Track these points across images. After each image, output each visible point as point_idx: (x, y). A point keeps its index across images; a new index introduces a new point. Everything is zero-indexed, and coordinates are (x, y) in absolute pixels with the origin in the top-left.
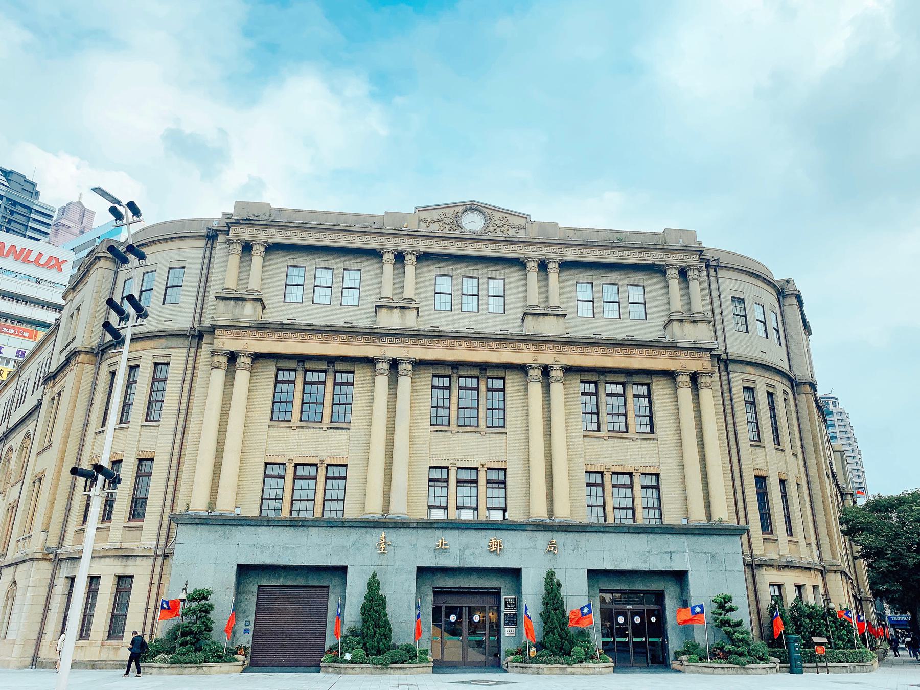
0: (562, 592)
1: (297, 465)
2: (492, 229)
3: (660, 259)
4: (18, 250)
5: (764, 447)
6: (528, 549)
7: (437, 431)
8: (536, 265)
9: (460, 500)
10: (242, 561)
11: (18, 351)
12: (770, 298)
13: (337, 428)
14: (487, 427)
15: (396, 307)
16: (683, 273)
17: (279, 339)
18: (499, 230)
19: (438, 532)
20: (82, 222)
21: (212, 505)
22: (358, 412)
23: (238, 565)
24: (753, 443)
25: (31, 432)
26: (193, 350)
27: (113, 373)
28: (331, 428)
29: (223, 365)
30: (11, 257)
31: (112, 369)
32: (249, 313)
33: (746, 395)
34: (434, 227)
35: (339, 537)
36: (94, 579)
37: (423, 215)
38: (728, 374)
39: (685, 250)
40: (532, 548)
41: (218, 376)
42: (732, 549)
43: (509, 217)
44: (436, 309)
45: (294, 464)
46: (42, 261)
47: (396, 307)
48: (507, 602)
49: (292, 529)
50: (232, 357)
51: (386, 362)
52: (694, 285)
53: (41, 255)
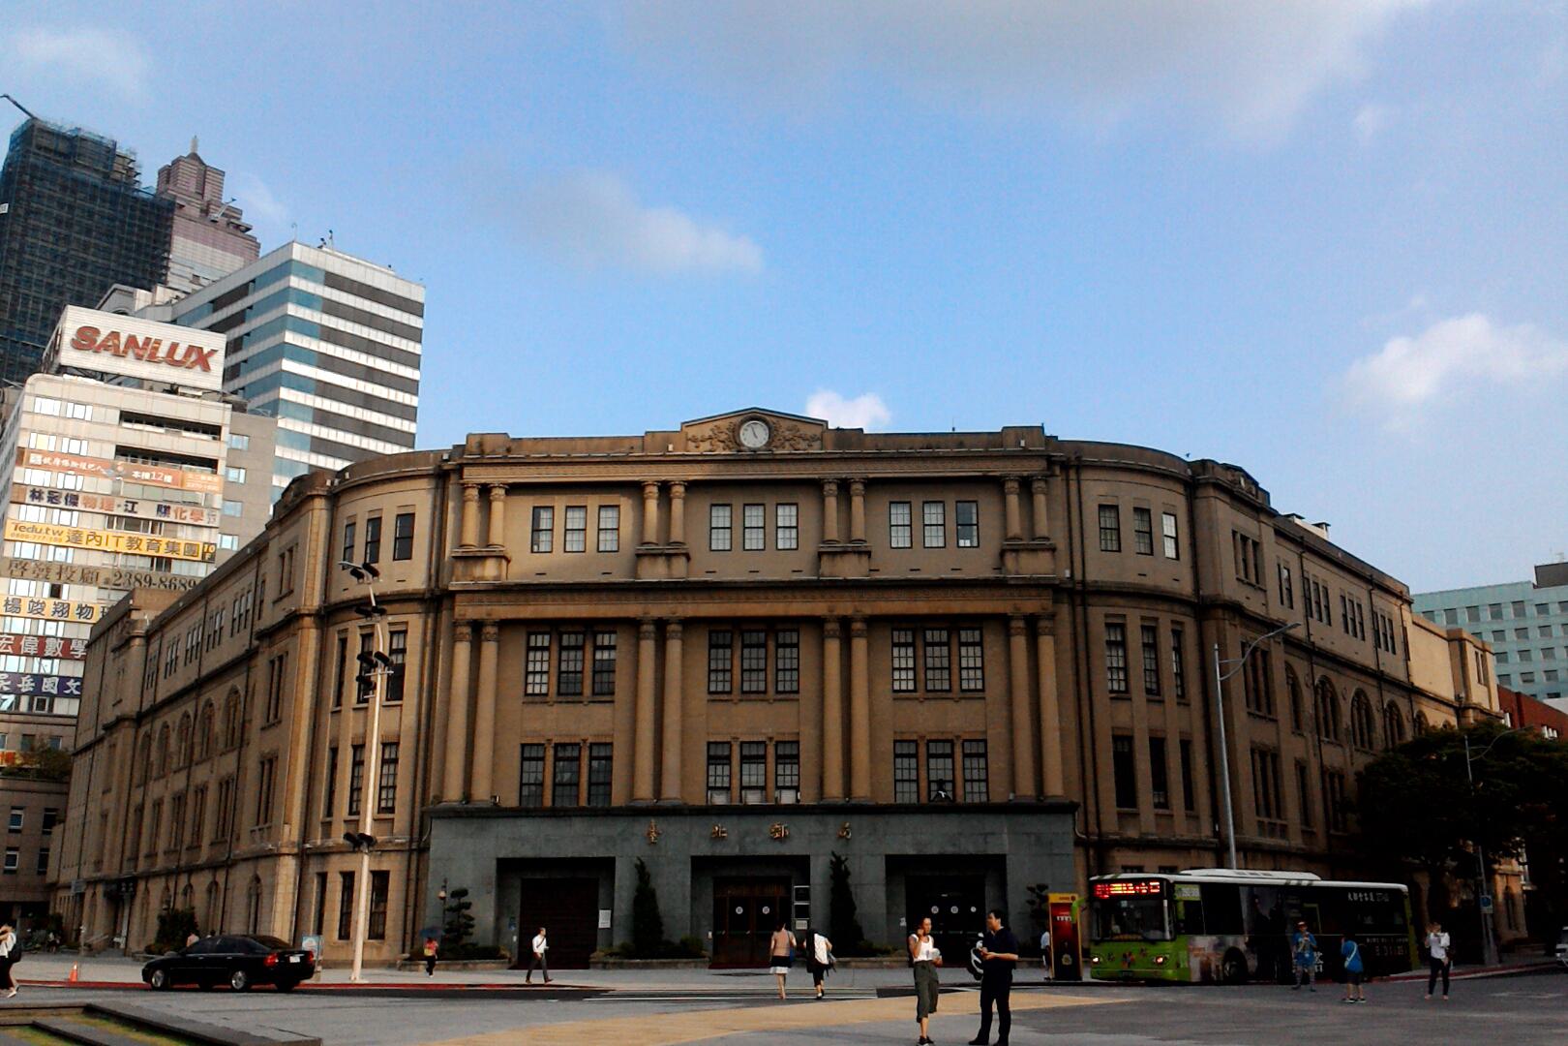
0: (851, 880)
1: (557, 746)
2: (778, 443)
3: (996, 469)
4: (140, 341)
5: (1130, 699)
9: (745, 779)
11: (159, 508)
12: (1164, 498)
14: (777, 692)
16: (1026, 485)
17: (527, 603)
18: (787, 444)
19: (714, 819)
20: (202, 195)
21: (467, 796)
22: (621, 682)
24: (1113, 695)
25: (239, 688)
26: (432, 615)
27: (343, 642)
30: (131, 354)
31: (343, 636)
32: (489, 570)
33: (1112, 634)
34: (705, 447)
35: (603, 829)
36: (349, 878)
37: (692, 432)
38: (1085, 610)
39: (1025, 455)
41: (463, 650)
42: (1064, 830)
43: (799, 425)
44: (713, 548)
46: (179, 355)
50: (477, 626)
52: (1040, 500)
53: (174, 347)
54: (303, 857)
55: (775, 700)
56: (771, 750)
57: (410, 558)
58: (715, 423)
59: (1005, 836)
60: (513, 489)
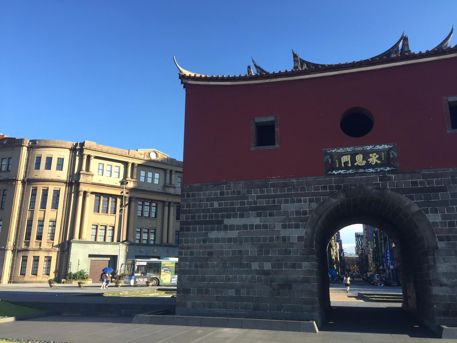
8: (169, 171)
10: (90, 254)
13: (112, 216)
15: (132, 181)
23: (89, 255)
28: (111, 215)
47: (132, 181)
50: (85, 193)
54: (13, 251)
55: (152, 219)
57: (50, 170)
58: (145, 151)
60: (96, 157)
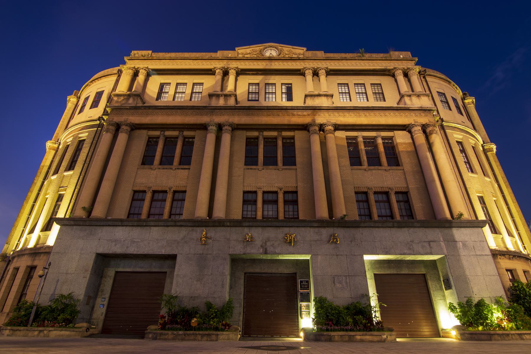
1: (154, 192)
6: (316, 241)
7: (248, 169)
13: (182, 169)
17: (147, 115)
28: (178, 169)
29: (111, 131)
40: (318, 240)
45: (151, 191)
48: (302, 284)
49: (139, 228)
51: (214, 126)
55: (283, 169)
56: (281, 196)
59: (442, 244)
